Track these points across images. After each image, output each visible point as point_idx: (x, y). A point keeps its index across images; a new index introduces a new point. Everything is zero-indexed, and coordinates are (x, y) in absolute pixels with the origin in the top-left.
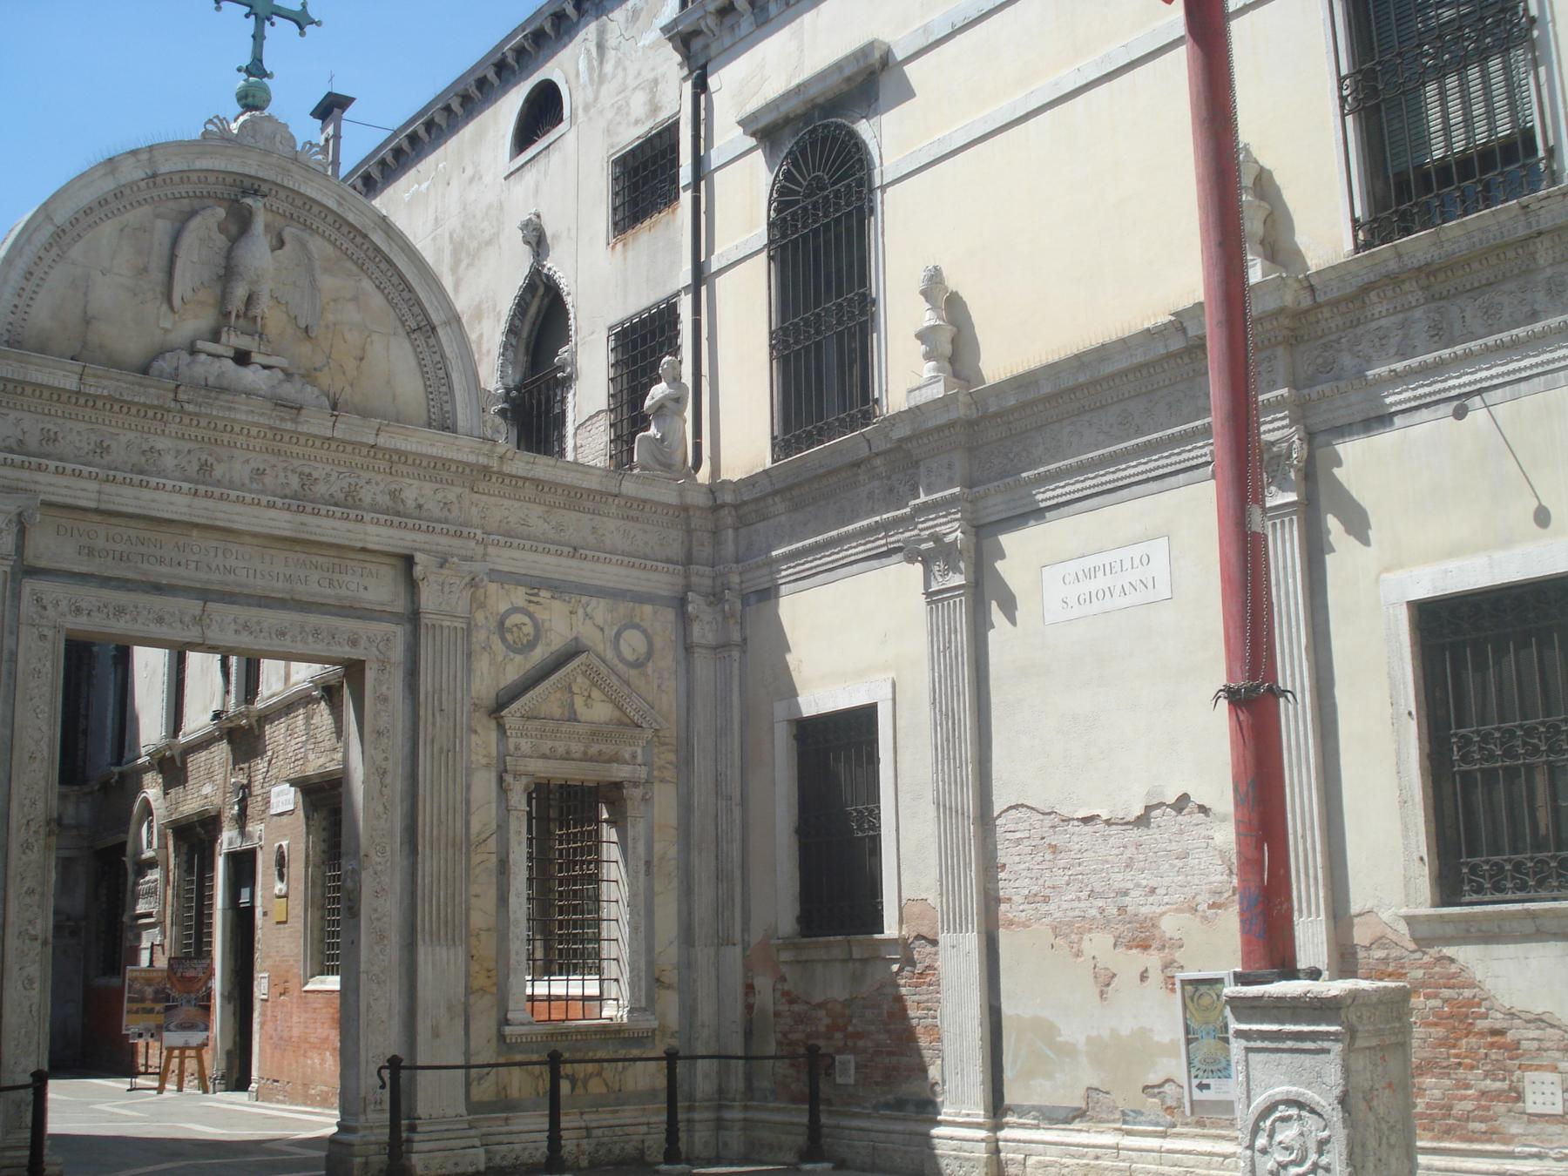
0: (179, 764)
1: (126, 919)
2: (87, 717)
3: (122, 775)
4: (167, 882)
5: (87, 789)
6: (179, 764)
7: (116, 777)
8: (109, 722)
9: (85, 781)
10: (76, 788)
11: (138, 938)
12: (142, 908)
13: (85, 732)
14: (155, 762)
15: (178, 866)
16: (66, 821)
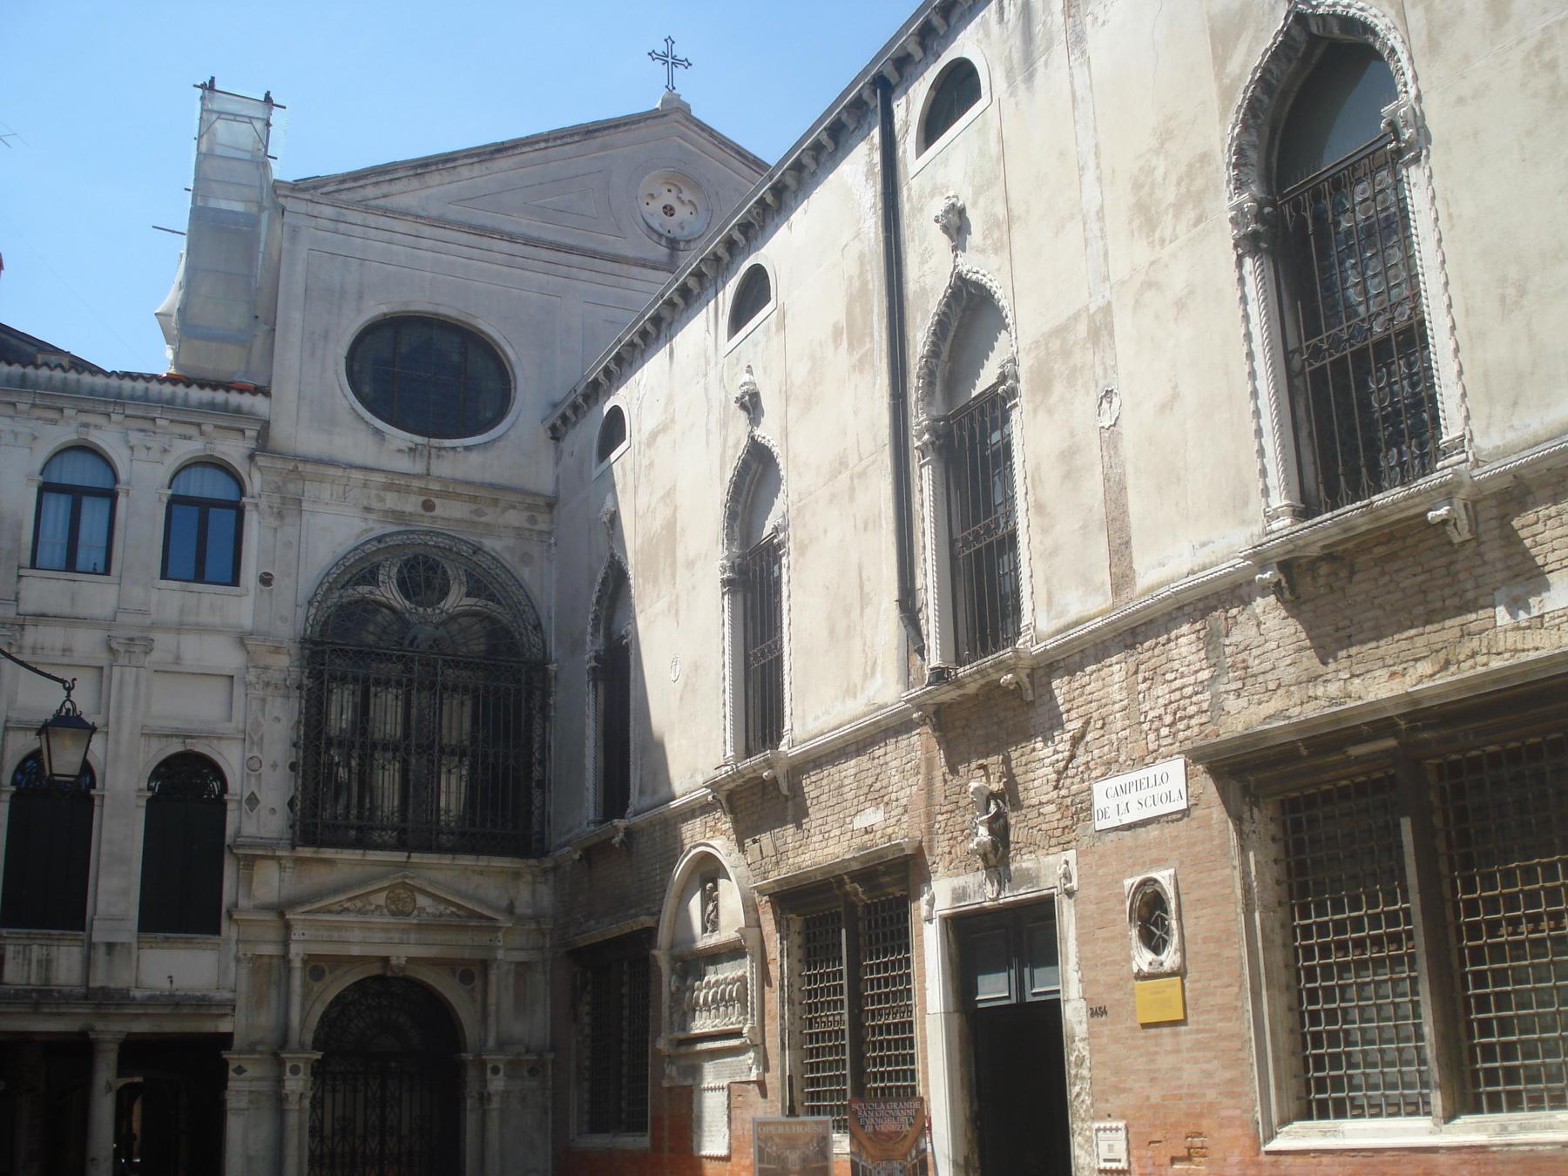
0: (785, 791)
1: (662, 1044)
2: (542, 763)
3: (629, 832)
4: (765, 978)
5: (548, 863)
6: (785, 791)
7: (621, 835)
8: (589, 763)
9: (543, 853)
10: (532, 862)
11: (695, 1072)
12: (702, 1024)
13: (542, 784)
14: (722, 797)
15: (787, 953)
16: (521, 909)
